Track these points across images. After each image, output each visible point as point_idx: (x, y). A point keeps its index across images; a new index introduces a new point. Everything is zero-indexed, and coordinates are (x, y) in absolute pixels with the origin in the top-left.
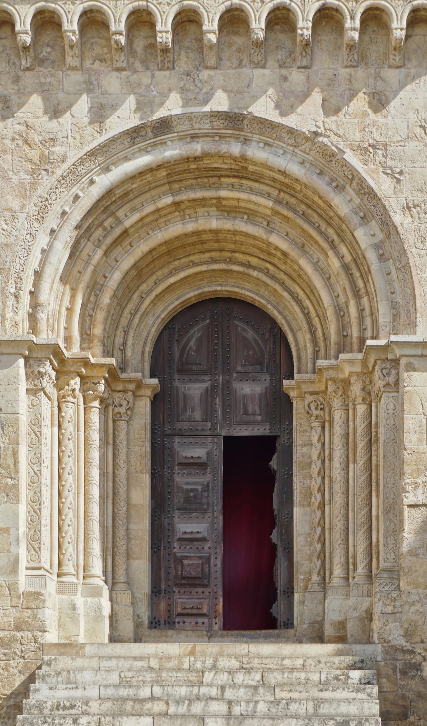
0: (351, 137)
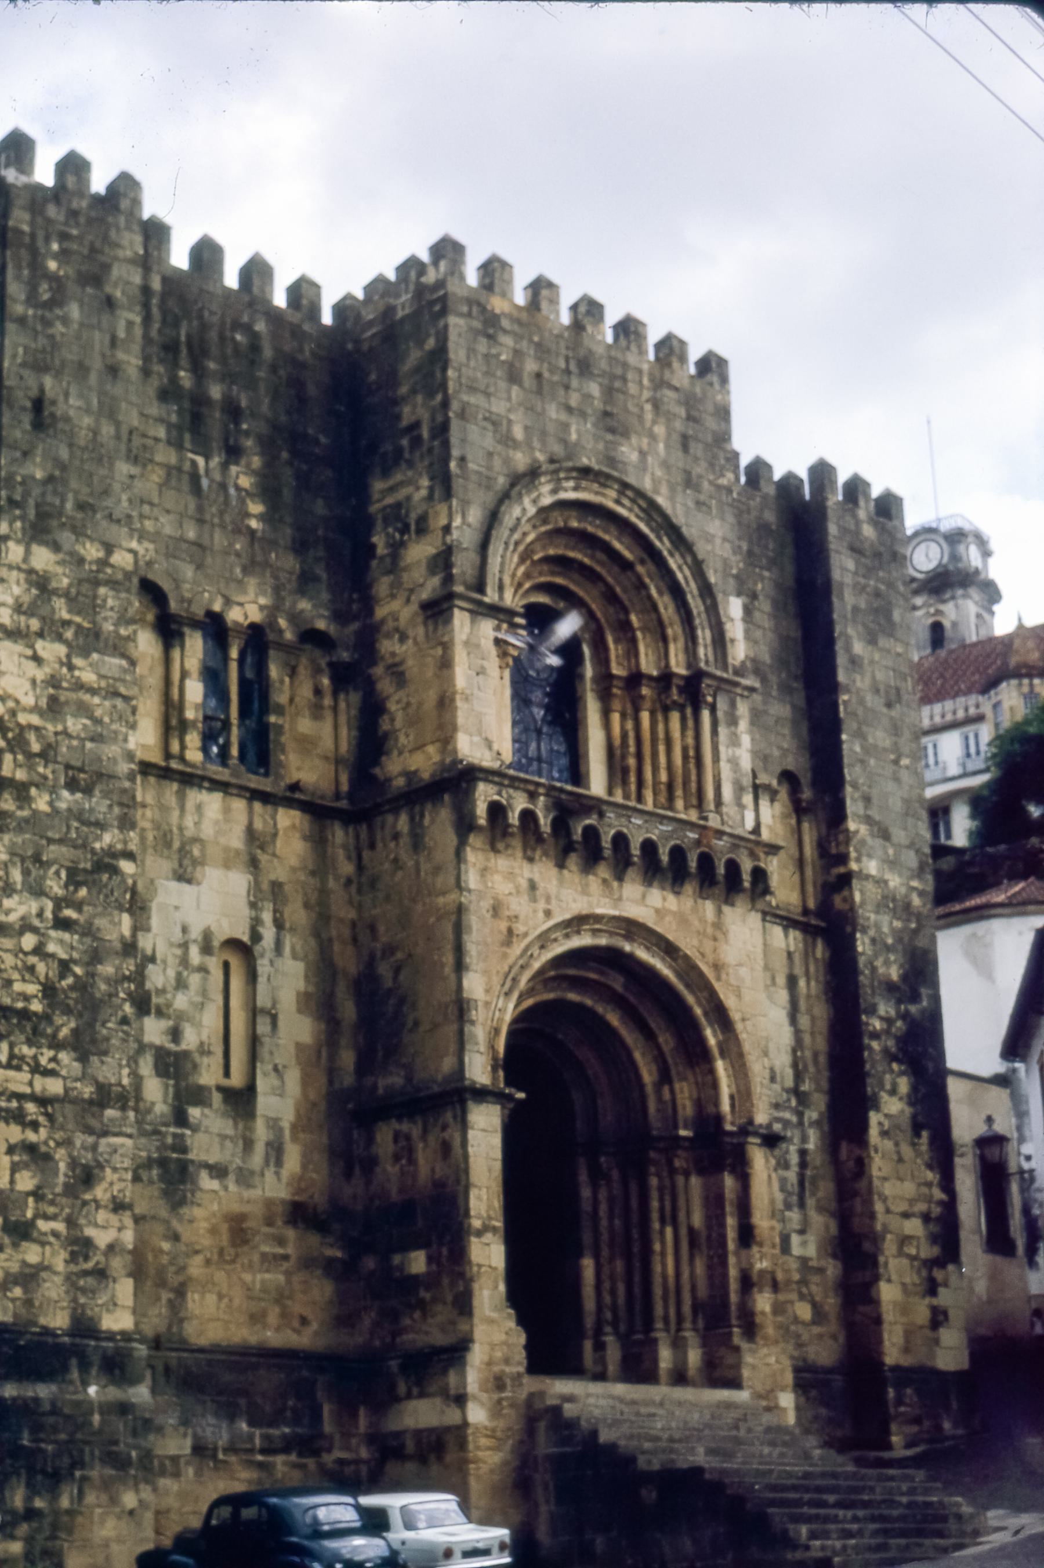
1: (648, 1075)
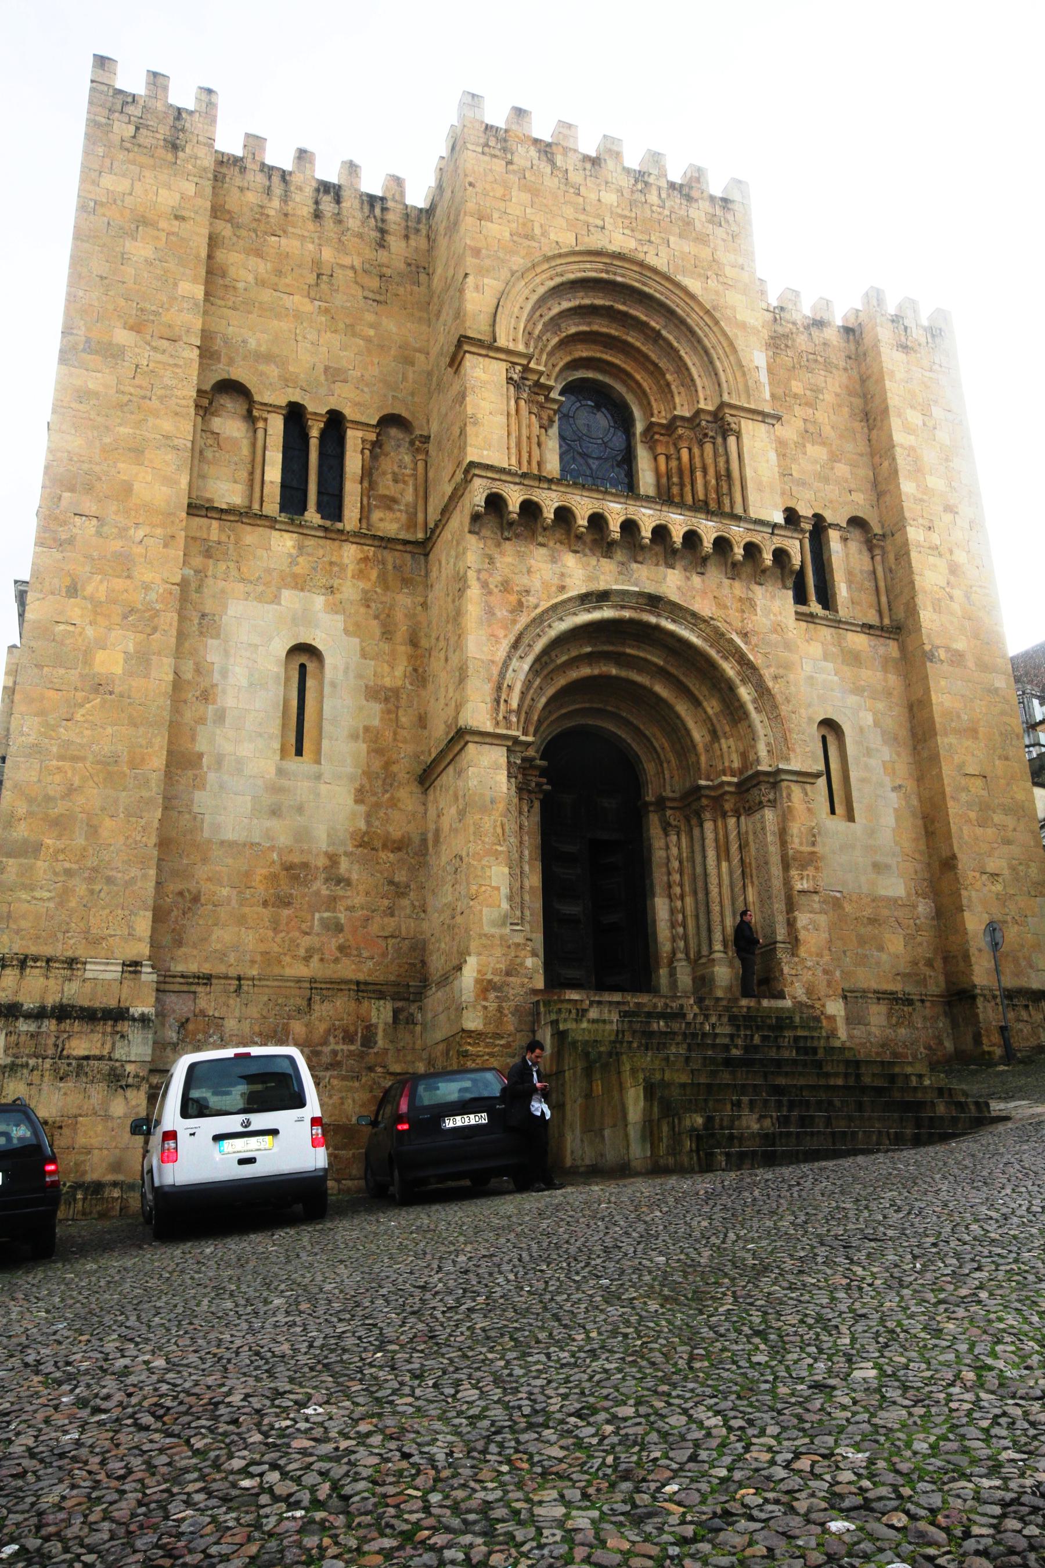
0: (734, 623)
1: (698, 735)
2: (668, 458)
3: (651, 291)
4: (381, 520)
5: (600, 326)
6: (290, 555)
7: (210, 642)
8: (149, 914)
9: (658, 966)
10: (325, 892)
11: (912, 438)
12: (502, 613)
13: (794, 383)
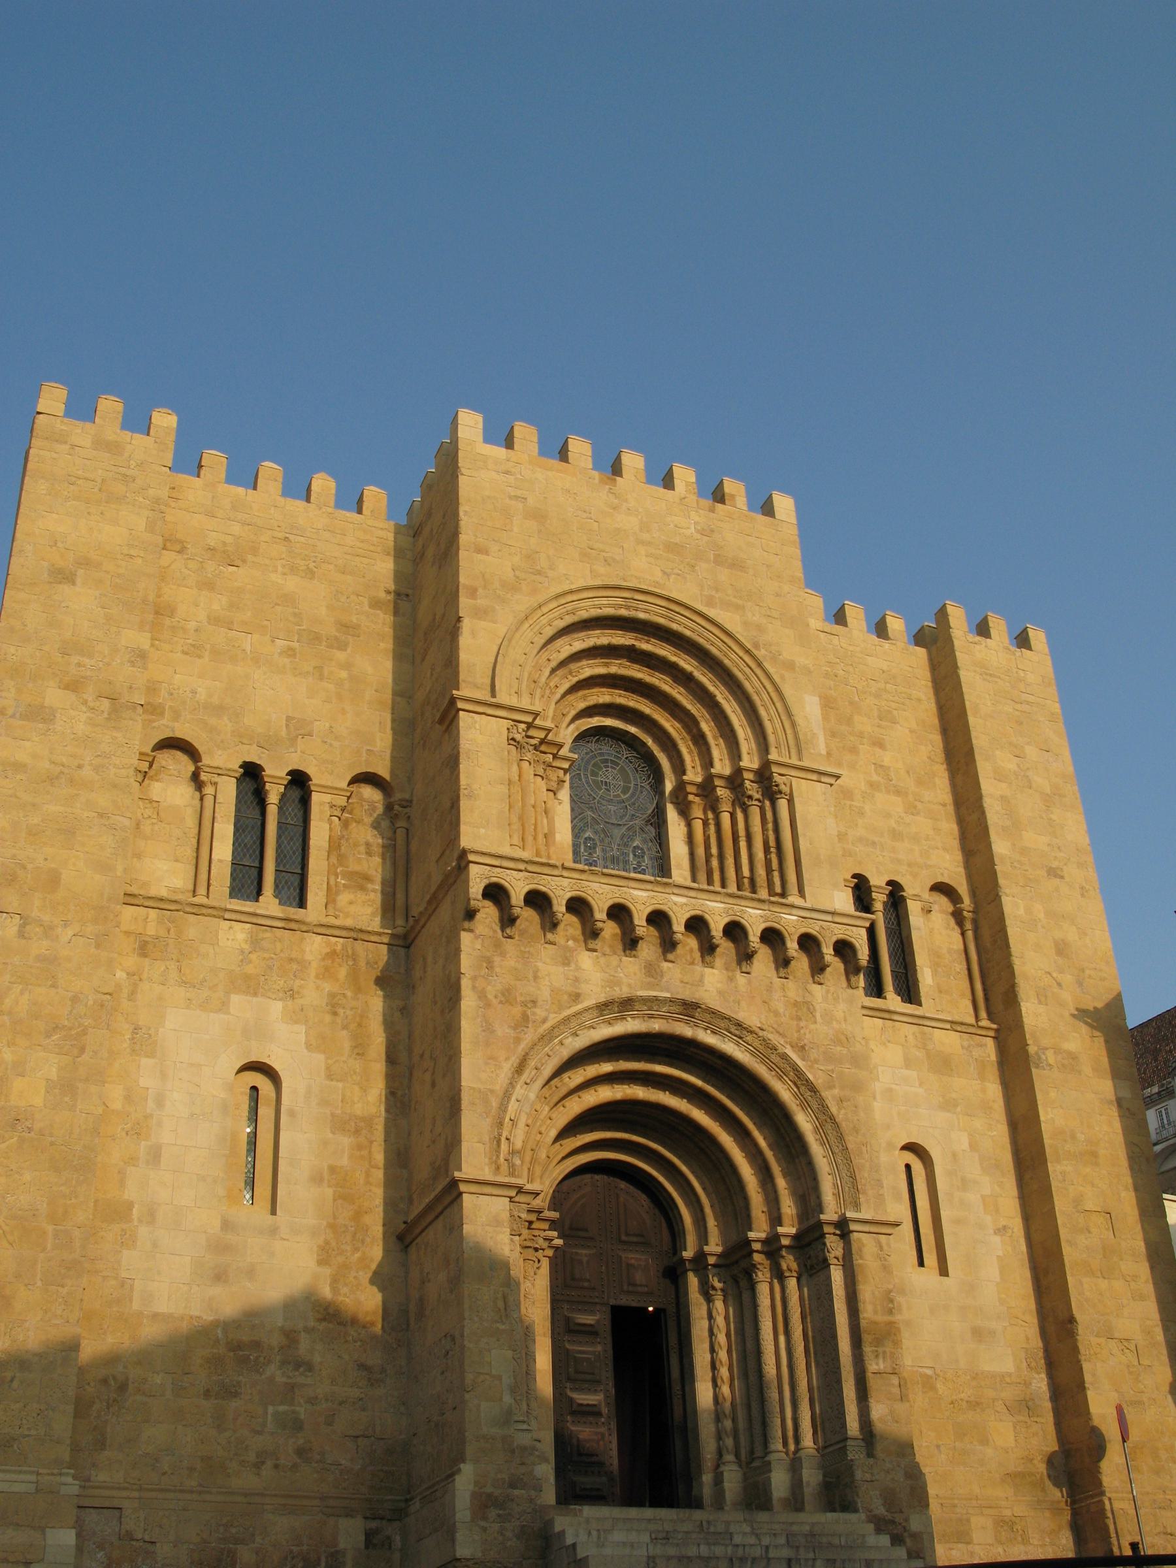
2: (705, 823)
3: (680, 629)
4: (351, 903)
5: (618, 667)
6: (242, 952)
7: (145, 1061)
8: (70, 1408)
9: (700, 1473)
10: (280, 1379)
11: (1004, 785)
12: (503, 1030)
13: (856, 718)
